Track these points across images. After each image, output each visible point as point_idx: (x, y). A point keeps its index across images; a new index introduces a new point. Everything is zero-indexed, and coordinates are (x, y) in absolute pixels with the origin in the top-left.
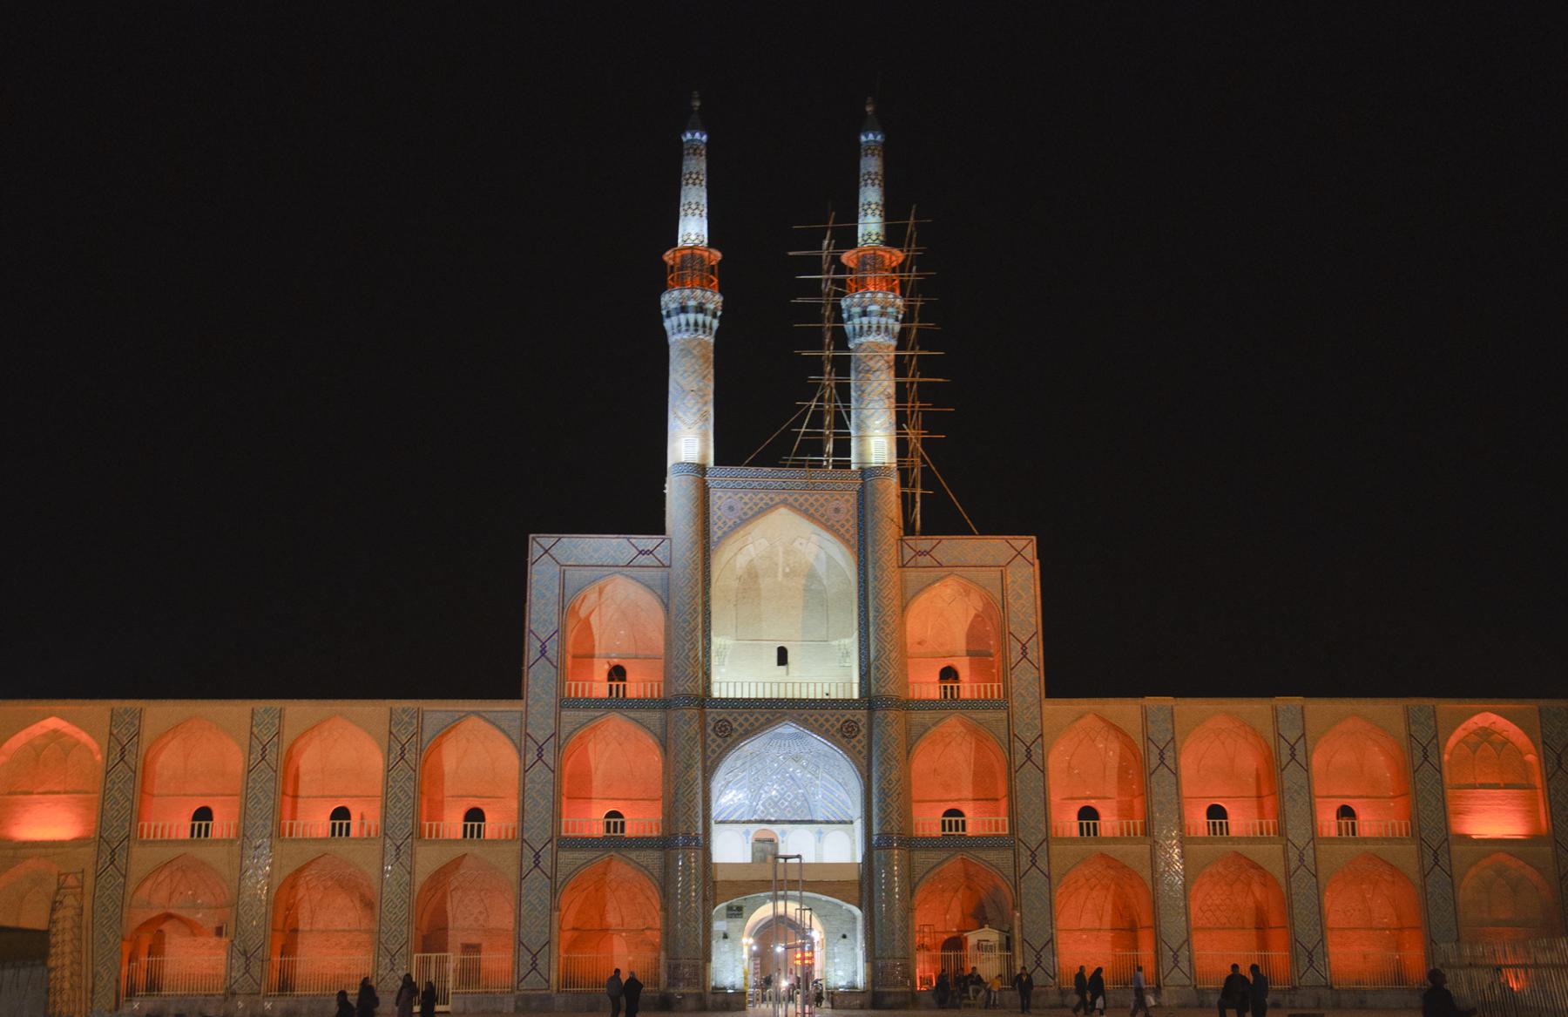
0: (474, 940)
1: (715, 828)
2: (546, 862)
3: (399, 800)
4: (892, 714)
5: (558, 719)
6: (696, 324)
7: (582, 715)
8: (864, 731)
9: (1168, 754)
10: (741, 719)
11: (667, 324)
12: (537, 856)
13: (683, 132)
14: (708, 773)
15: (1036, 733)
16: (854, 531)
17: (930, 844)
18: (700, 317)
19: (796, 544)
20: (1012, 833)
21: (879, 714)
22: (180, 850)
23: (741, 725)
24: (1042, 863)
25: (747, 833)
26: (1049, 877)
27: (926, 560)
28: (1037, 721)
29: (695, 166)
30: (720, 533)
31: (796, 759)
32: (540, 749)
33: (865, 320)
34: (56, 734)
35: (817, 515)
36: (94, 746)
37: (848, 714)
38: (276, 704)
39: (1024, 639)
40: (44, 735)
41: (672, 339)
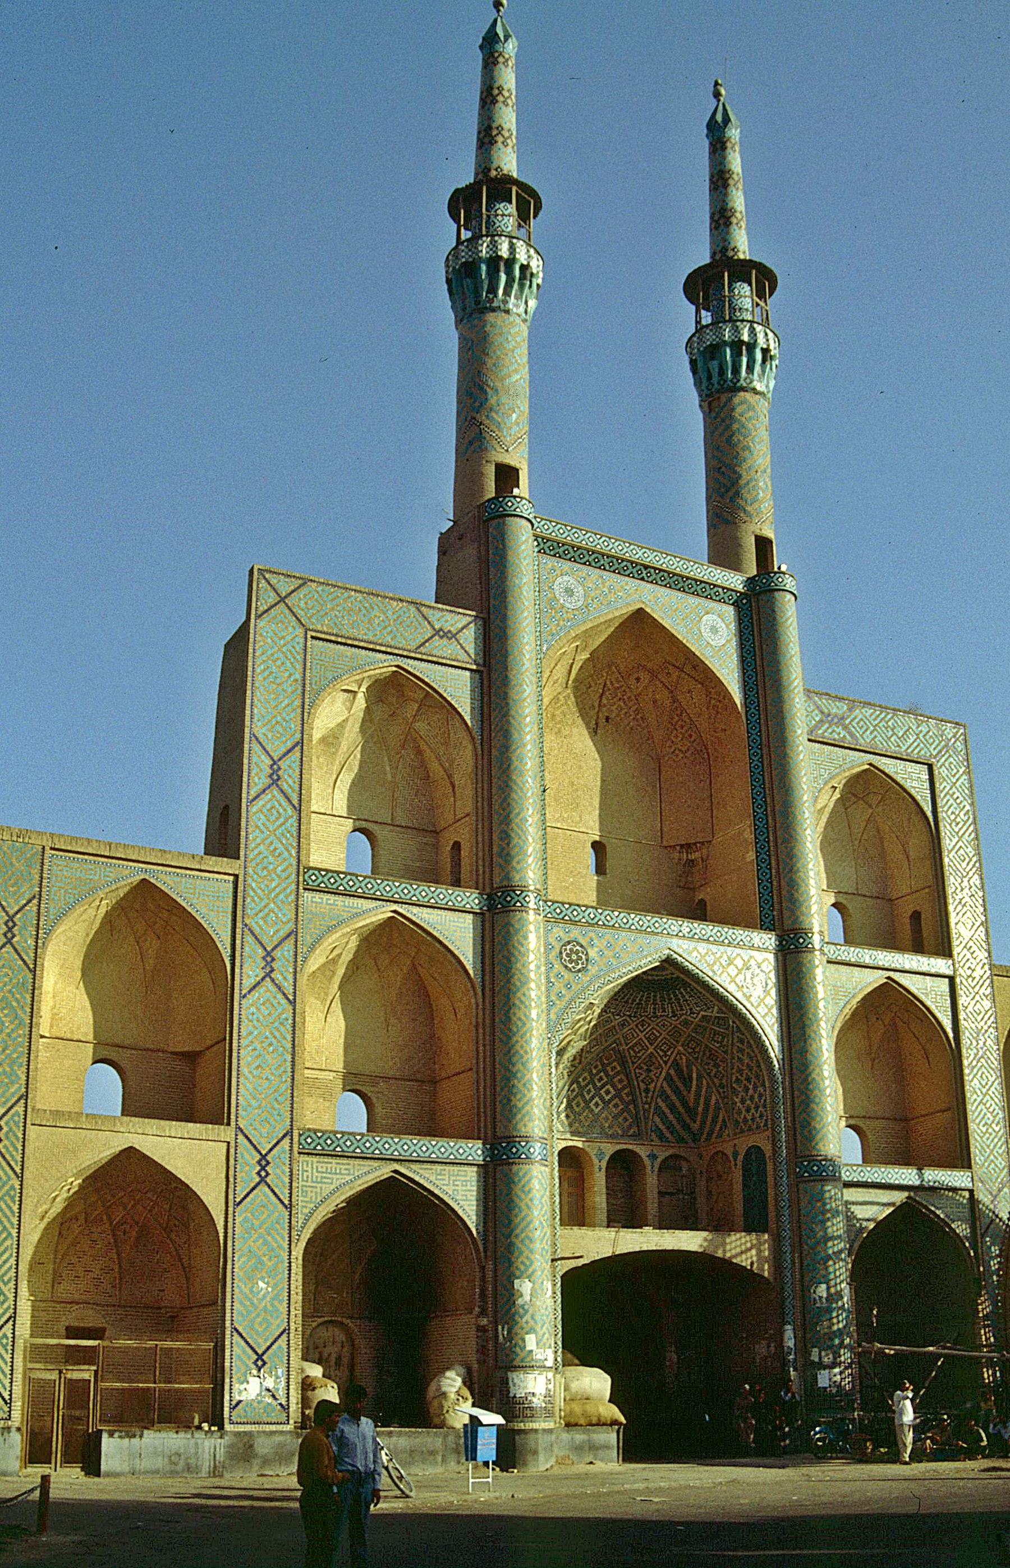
2: (278, 1175)
12: (263, 1162)
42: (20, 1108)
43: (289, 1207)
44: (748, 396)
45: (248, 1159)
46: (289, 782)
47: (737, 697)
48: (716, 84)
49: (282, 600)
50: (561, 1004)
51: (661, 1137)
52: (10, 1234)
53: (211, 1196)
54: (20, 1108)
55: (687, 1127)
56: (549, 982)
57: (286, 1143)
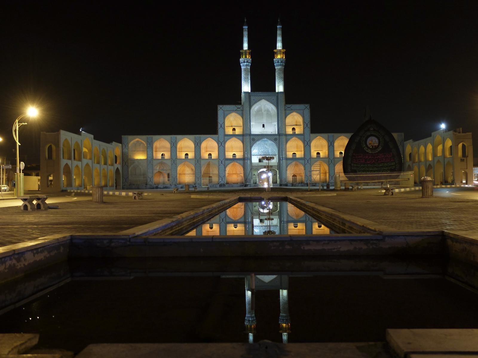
0: (211, 176)
1: (252, 156)
2: (223, 162)
4: (283, 137)
5: (224, 139)
6: (247, 65)
7: (228, 137)
8: (278, 140)
9: (332, 143)
10: (257, 138)
11: (241, 65)
13: (243, 26)
14: (251, 147)
16: (276, 104)
17: (290, 159)
18: (247, 63)
19: (266, 106)
20: (304, 157)
21: (281, 137)
22: (161, 161)
24: (309, 162)
25: (258, 157)
27: (290, 109)
28: (309, 138)
29: (245, 34)
31: (266, 144)
33: (278, 63)
34: (138, 141)
36: (145, 143)
37: (275, 137)
38: (175, 136)
40: (136, 141)
41: (242, 68)
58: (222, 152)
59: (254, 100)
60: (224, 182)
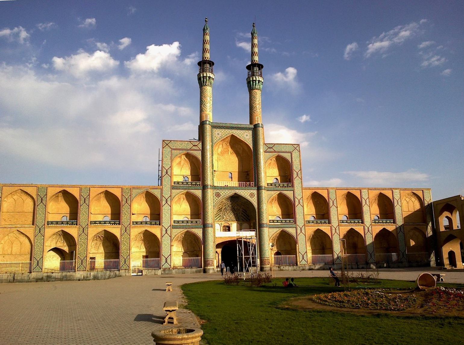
2: (169, 232)
3: (126, 215)
8: (256, 196)
9: (335, 202)
10: (223, 192)
12: (166, 230)
15: (302, 196)
23: (223, 194)
24: (303, 231)
26: (305, 235)
27: (272, 150)
30: (215, 141)
32: (167, 200)
35: (242, 137)
39: (297, 171)
42: (129, 226)
43: (170, 237)
44: (256, 90)
45: (164, 230)
46: (169, 173)
47: (251, 146)
48: (254, 24)
49: (167, 145)
50: (215, 202)
51: (243, 220)
52: (128, 244)
53: (159, 236)
54: (129, 226)
55: (248, 218)
56: (213, 199)
57: (170, 227)
58: (167, 215)
59: (218, 134)
60: (170, 266)
